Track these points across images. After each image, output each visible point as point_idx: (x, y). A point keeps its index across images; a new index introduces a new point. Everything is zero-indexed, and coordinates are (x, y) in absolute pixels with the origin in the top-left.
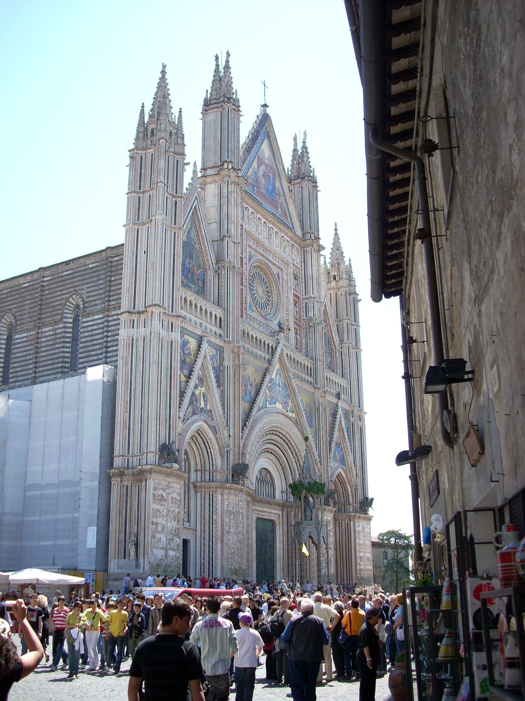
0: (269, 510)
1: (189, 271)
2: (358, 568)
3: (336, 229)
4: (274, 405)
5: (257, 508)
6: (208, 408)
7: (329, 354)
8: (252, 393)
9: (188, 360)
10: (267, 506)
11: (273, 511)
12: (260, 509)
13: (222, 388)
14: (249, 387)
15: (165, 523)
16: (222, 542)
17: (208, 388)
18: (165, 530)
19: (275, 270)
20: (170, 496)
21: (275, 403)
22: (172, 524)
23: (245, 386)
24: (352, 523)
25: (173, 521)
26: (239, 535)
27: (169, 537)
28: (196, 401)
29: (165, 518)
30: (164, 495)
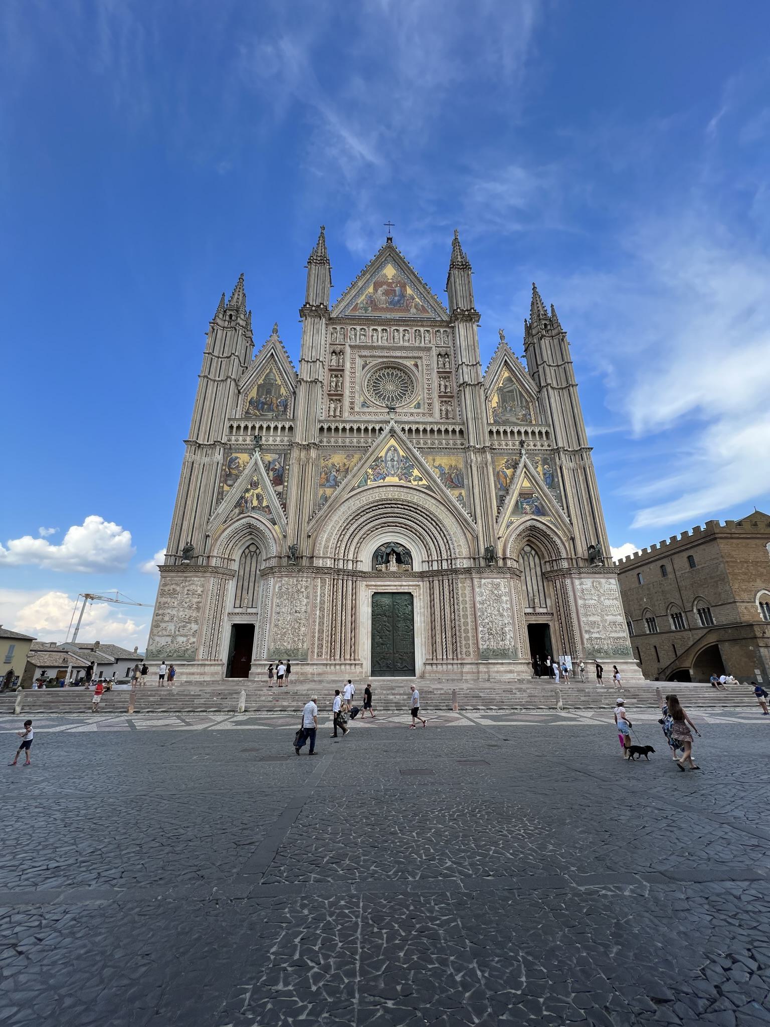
0: (400, 583)
1: (264, 404)
2: (586, 636)
3: (534, 288)
4: (382, 481)
5: (373, 583)
6: (265, 504)
7: (522, 407)
8: (339, 478)
9: (234, 472)
10: (395, 579)
11: (404, 583)
12: (379, 583)
13: (286, 484)
14: (334, 473)
15: (175, 613)
16: (270, 623)
17: (265, 488)
18: (175, 619)
19: (409, 363)
20: (186, 589)
21: (384, 479)
22: (186, 613)
23: (326, 474)
24: (568, 581)
25: (187, 610)
26: (297, 614)
27: (180, 624)
28: (246, 502)
29: (176, 609)
30: (178, 588)
